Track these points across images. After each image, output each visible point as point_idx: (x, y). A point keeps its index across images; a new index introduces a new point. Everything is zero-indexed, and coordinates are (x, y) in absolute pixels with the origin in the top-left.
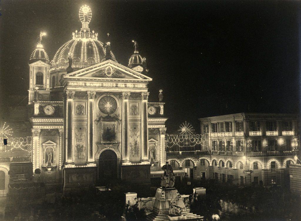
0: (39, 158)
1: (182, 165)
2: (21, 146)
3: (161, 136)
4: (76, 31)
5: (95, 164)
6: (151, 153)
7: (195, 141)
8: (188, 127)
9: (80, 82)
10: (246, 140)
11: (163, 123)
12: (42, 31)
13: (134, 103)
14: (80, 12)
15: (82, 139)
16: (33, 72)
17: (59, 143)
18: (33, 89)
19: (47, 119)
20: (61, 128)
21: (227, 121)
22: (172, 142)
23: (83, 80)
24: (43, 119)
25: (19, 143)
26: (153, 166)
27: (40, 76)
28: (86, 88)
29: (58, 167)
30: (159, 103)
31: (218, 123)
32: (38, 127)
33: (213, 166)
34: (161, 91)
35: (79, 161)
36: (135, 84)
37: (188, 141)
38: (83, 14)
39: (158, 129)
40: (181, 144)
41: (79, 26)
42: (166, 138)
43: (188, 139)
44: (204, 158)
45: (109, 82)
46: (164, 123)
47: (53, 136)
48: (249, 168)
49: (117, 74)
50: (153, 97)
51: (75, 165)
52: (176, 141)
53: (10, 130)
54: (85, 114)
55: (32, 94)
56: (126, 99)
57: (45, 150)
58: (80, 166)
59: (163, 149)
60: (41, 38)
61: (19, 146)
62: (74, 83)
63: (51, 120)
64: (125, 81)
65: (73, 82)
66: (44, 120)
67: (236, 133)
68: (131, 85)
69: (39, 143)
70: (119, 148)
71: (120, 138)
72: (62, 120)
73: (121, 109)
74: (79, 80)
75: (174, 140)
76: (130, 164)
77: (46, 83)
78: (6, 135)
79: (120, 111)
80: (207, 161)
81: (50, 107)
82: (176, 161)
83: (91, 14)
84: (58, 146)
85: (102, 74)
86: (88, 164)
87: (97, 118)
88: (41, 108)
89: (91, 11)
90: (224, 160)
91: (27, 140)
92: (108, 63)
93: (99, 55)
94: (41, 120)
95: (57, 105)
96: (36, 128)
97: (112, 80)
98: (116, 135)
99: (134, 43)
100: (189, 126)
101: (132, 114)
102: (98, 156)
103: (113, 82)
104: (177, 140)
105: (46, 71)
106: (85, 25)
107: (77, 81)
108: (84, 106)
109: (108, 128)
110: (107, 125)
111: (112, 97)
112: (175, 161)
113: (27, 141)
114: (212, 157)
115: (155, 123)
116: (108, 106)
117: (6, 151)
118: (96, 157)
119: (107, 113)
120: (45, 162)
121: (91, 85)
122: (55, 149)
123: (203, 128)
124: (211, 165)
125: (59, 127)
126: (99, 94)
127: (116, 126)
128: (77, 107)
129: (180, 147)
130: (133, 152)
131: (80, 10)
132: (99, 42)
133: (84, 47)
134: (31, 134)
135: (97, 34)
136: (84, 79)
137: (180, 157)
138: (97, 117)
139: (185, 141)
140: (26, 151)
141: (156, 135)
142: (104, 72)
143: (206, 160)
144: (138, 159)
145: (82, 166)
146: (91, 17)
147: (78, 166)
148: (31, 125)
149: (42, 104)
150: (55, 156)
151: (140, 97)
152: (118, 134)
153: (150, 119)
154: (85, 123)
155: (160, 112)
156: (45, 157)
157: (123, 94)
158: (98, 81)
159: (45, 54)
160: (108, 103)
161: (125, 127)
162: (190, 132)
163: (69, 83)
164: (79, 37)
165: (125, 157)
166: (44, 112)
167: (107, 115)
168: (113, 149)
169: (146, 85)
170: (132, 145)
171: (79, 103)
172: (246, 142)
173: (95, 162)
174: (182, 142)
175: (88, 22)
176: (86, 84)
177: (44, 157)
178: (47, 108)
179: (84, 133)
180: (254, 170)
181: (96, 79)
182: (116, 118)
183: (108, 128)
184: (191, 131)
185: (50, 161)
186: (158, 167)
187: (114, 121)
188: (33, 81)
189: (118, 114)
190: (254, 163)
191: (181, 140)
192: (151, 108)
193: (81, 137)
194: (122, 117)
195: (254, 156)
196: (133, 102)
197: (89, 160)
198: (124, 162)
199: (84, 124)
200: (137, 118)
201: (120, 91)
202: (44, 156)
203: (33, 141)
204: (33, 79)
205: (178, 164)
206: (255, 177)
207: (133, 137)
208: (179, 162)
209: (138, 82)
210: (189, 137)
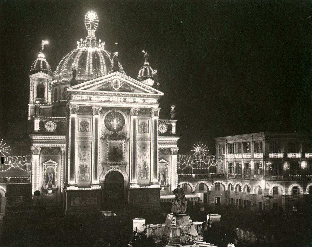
0: (39, 179)
1: (195, 189)
2: (20, 165)
3: (172, 157)
4: (82, 40)
5: (100, 186)
6: (161, 175)
7: (210, 163)
8: (202, 147)
9: (84, 96)
10: (265, 162)
11: (175, 142)
12: (45, 40)
13: (142, 120)
14: (85, 18)
15: (86, 159)
16: (34, 84)
17: (60, 163)
18: (33, 103)
19: (48, 136)
20: (63, 146)
21: (245, 141)
22: (185, 164)
23: (88, 93)
24: (43, 136)
25: (18, 162)
26: (163, 190)
27: (41, 89)
28: (90, 102)
29: (59, 190)
30: (171, 120)
31: (235, 143)
32: (39, 144)
33: (229, 191)
34: (173, 107)
35: (82, 183)
36: (144, 98)
37: (202, 163)
38: (90, 21)
39: (170, 149)
40: (195, 166)
41: (84, 34)
42: (178, 159)
43: (201, 161)
44: (219, 181)
45: (116, 96)
46: (176, 142)
47: (54, 155)
48: (268, 193)
49: (126, 88)
50: (164, 114)
51: (78, 188)
52: (189, 162)
53: (7, 147)
54: (89, 131)
55: (32, 108)
56: (134, 115)
57: (46, 170)
58: (83, 189)
59: (174, 172)
60: (43, 47)
61: (17, 166)
62: (77, 97)
63: (52, 137)
64: (134, 95)
65: (78, 95)
66: (45, 137)
67: (254, 154)
68: (141, 99)
69: (39, 163)
70: (126, 169)
71: (127, 157)
72: (64, 137)
73: (129, 127)
74: (83, 93)
75: (187, 161)
76: (138, 187)
77: (47, 97)
78: (4, 153)
79: (128, 129)
80: (223, 185)
81: (51, 123)
82: (188, 184)
83: (98, 21)
84: (60, 166)
85: (109, 88)
86: (92, 186)
87: (103, 136)
88: (42, 124)
89: (97, 18)
90: (241, 184)
91: (26, 159)
92: (115, 75)
93: (106, 66)
94: (42, 137)
95: (59, 121)
96: (36, 146)
97: (120, 94)
98: (123, 155)
99: (144, 54)
100: (203, 146)
101: (142, 132)
102: (103, 178)
103: (121, 96)
104: (190, 162)
105: (48, 83)
106: (91, 33)
107: (81, 94)
108: (89, 122)
109: (114, 146)
110: (113, 143)
111: (120, 113)
112: (187, 184)
113: (26, 161)
114: (228, 180)
115: (166, 142)
116: (115, 123)
117: (3, 171)
118: (101, 179)
119: (114, 130)
120: (45, 184)
121: (97, 99)
122: (56, 169)
123: (218, 148)
124: (227, 189)
125: (61, 145)
126: (105, 109)
127: (123, 145)
128: (81, 123)
129: (193, 170)
130: (142, 174)
131: (86, 16)
132: (106, 52)
133: (90, 57)
134: (30, 152)
135: (104, 43)
136: (89, 93)
137: (193, 181)
138: (103, 134)
139: (198, 162)
140: (25, 171)
141: (167, 156)
142: (111, 85)
143: (221, 183)
144: (147, 182)
145: (86, 189)
146: (98, 24)
147: (81, 189)
148: (31, 142)
149: (43, 120)
150: (56, 176)
151: (151, 113)
152: (126, 154)
153: (160, 138)
154: (89, 141)
155: (171, 130)
156: (45, 178)
157: (132, 109)
158: (104, 95)
159: (47, 64)
160: (115, 119)
161: (133, 146)
162: (204, 153)
163: (72, 96)
164: (84, 46)
165: (133, 180)
166: (44, 128)
167: (114, 132)
168: (120, 171)
169: (157, 100)
170: (140, 166)
171: (84, 119)
172: (265, 165)
173: (100, 185)
174: (196, 164)
175: (95, 29)
176: (92, 99)
177: (44, 178)
178: (48, 124)
179: (89, 153)
180: (274, 196)
181: (102, 93)
182: (123, 137)
183: (114, 146)
184: (206, 152)
185: (51, 182)
186: (169, 191)
187: (122, 139)
188: (34, 94)
189: (125, 132)
190: (274, 188)
191: (194, 162)
192: (162, 125)
193: (85, 156)
194: (130, 135)
195: (274, 181)
196: (143, 119)
197: (94, 182)
198: (131, 185)
199: (88, 142)
200: (147, 136)
201: (129, 107)
202: (44, 176)
203: (33, 160)
204: (34, 92)
205: (190, 187)
206: (274, 204)
207: (142, 158)
208: (192, 186)
209: (148, 96)
210: (203, 158)
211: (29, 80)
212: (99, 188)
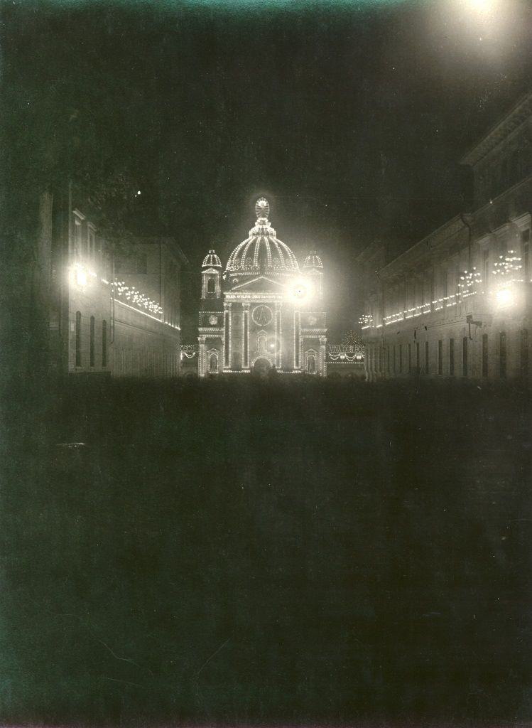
96: (201, 338)
148: (198, 334)
211: (201, 276)
212: (248, 371)
